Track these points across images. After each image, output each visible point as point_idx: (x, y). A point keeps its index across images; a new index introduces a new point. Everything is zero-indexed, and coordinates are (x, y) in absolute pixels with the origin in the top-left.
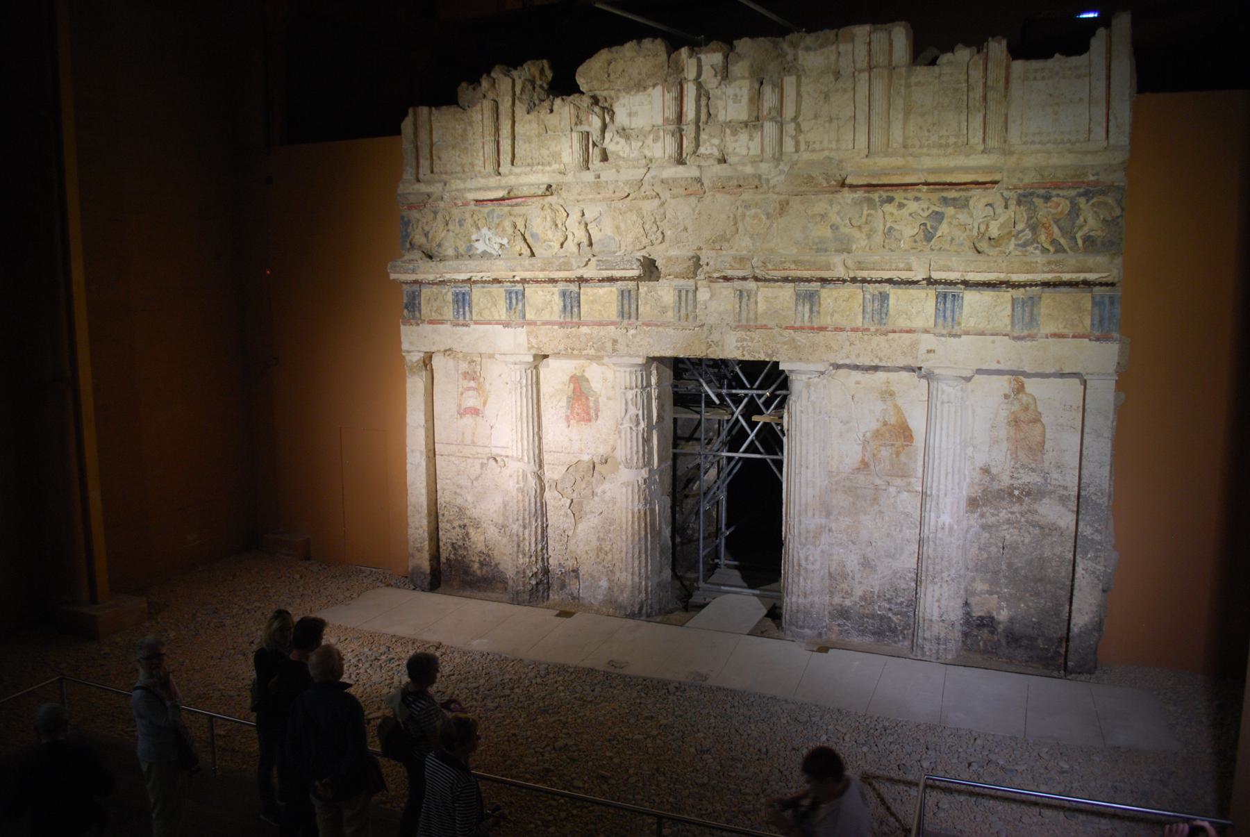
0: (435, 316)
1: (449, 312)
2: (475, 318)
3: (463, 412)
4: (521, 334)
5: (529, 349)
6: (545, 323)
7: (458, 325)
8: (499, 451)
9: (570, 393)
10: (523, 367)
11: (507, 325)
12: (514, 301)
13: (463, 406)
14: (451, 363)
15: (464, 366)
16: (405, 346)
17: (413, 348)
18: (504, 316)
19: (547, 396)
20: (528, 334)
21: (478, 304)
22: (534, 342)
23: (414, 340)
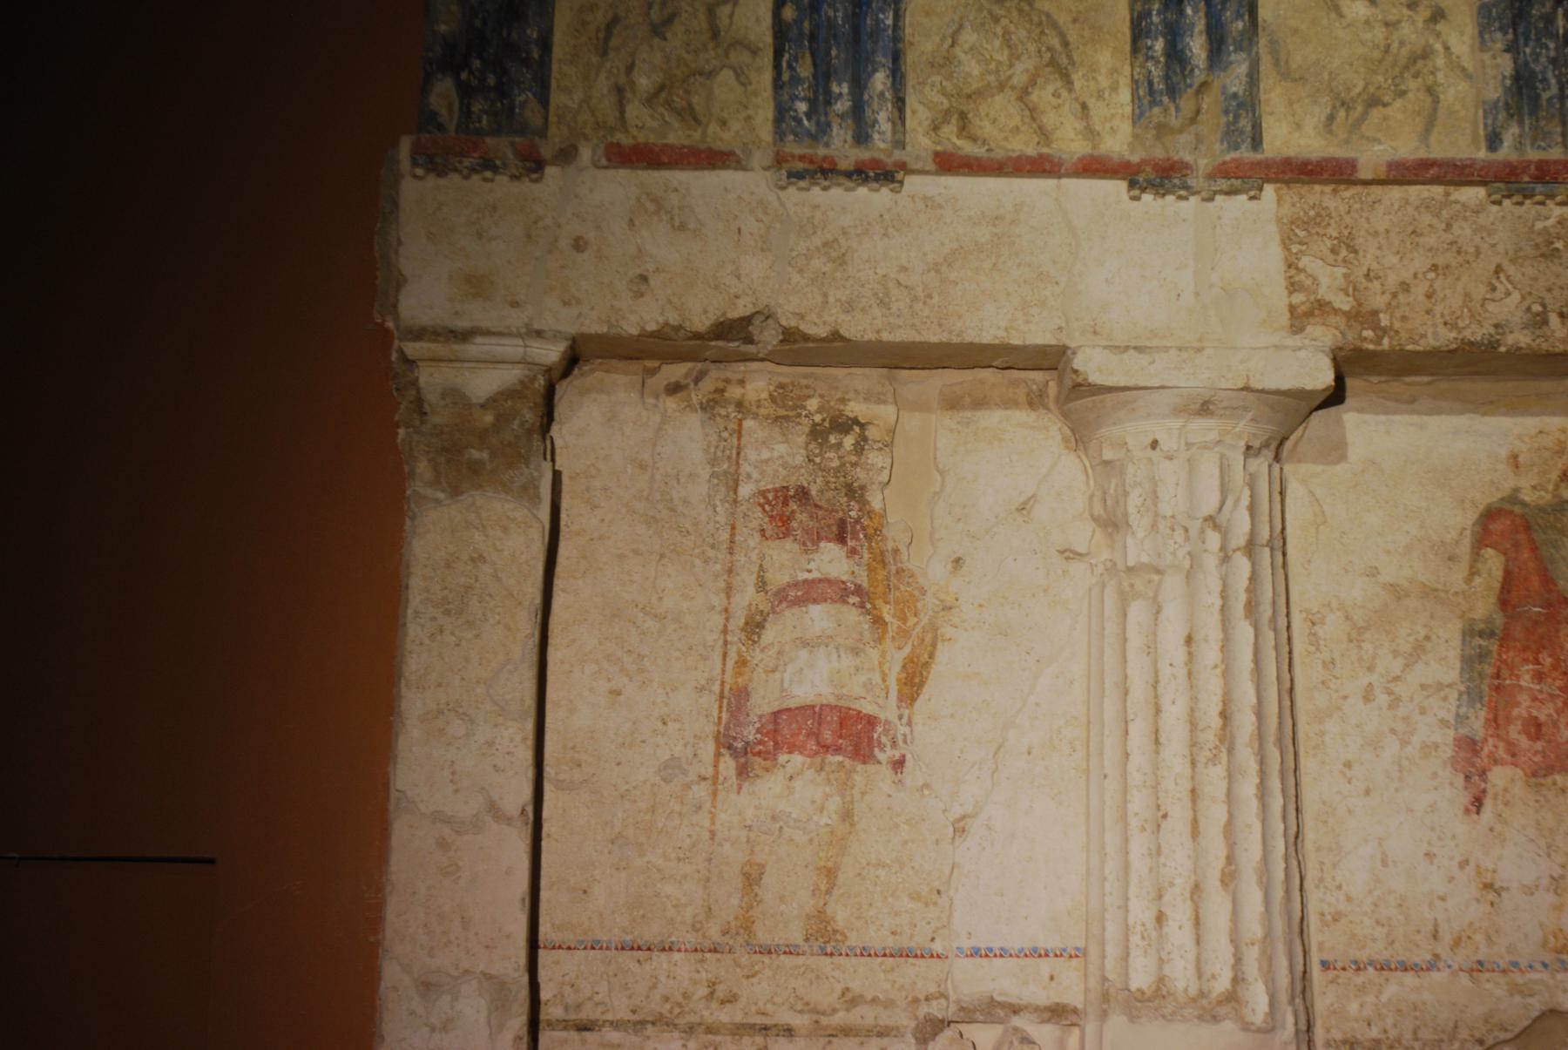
0: (643, 124)
1: (745, 104)
2: (921, 142)
3: (755, 740)
4: (1249, 230)
5: (1298, 320)
6: (1404, 174)
7: (825, 172)
8: (1002, 981)
9: (1484, 607)
10: (1244, 429)
11: (1158, 177)
12: (1197, 47)
13: (763, 702)
14: (688, 438)
15: (775, 455)
16: (424, 297)
17: (476, 314)
18: (1118, 142)
19: (1333, 626)
20: (1294, 234)
21: (944, 63)
22: (1328, 279)
23: (480, 268)
